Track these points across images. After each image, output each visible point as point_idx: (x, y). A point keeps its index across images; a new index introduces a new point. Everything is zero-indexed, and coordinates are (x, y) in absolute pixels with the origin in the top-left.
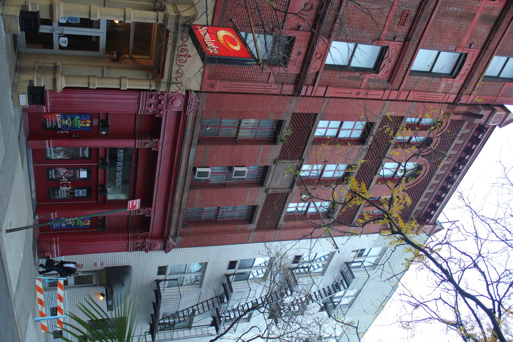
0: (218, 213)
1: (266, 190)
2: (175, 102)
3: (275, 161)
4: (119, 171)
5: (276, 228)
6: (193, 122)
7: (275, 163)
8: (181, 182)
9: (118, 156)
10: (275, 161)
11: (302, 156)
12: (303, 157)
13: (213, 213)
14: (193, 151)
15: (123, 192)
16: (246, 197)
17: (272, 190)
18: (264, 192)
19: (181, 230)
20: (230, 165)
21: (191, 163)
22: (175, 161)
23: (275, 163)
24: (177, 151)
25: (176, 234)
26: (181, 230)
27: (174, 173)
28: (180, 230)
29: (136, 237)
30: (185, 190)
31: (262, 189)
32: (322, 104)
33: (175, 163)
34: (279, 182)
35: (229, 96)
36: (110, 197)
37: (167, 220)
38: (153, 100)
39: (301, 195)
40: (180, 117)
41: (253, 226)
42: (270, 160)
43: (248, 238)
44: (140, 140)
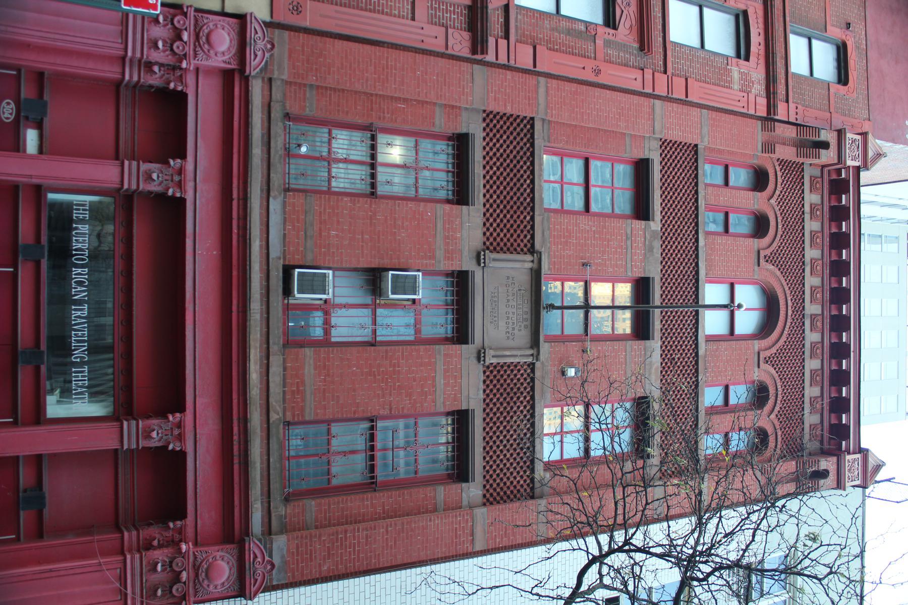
0: (372, 458)
1: (479, 353)
2: (214, 38)
3: (478, 255)
4: (79, 302)
5: (532, 497)
6: (265, 117)
7: (479, 264)
8: (258, 316)
9: (75, 245)
10: (478, 255)
11: (533, 245)
12: (537, 246)
13: (360, 466)
14: (275, 205)
15: (95, 394)
16: (434, 378)
17: (492, 352)
18: (475, 361)
19: (282, 510)
22: (235, 230)
23: (479, 264)
24: (235, 195)
25: (268, 531)
26: (282, 510)
27: (235, 273)
28: (279, 510)
29: (149, 547)
30: (274, 348)
31: (467, 350)
32: (537, 92)
33: (235, 237)
34: (502, 324)
35: (339, 44)
36: (55, 408)
37: (236, 461)
38: (160, 32)
39: (563, 373)
40: (233, 79)
41: (473, 491)
42: (465, 253)
43: (472, 534)
44: (135, 163)
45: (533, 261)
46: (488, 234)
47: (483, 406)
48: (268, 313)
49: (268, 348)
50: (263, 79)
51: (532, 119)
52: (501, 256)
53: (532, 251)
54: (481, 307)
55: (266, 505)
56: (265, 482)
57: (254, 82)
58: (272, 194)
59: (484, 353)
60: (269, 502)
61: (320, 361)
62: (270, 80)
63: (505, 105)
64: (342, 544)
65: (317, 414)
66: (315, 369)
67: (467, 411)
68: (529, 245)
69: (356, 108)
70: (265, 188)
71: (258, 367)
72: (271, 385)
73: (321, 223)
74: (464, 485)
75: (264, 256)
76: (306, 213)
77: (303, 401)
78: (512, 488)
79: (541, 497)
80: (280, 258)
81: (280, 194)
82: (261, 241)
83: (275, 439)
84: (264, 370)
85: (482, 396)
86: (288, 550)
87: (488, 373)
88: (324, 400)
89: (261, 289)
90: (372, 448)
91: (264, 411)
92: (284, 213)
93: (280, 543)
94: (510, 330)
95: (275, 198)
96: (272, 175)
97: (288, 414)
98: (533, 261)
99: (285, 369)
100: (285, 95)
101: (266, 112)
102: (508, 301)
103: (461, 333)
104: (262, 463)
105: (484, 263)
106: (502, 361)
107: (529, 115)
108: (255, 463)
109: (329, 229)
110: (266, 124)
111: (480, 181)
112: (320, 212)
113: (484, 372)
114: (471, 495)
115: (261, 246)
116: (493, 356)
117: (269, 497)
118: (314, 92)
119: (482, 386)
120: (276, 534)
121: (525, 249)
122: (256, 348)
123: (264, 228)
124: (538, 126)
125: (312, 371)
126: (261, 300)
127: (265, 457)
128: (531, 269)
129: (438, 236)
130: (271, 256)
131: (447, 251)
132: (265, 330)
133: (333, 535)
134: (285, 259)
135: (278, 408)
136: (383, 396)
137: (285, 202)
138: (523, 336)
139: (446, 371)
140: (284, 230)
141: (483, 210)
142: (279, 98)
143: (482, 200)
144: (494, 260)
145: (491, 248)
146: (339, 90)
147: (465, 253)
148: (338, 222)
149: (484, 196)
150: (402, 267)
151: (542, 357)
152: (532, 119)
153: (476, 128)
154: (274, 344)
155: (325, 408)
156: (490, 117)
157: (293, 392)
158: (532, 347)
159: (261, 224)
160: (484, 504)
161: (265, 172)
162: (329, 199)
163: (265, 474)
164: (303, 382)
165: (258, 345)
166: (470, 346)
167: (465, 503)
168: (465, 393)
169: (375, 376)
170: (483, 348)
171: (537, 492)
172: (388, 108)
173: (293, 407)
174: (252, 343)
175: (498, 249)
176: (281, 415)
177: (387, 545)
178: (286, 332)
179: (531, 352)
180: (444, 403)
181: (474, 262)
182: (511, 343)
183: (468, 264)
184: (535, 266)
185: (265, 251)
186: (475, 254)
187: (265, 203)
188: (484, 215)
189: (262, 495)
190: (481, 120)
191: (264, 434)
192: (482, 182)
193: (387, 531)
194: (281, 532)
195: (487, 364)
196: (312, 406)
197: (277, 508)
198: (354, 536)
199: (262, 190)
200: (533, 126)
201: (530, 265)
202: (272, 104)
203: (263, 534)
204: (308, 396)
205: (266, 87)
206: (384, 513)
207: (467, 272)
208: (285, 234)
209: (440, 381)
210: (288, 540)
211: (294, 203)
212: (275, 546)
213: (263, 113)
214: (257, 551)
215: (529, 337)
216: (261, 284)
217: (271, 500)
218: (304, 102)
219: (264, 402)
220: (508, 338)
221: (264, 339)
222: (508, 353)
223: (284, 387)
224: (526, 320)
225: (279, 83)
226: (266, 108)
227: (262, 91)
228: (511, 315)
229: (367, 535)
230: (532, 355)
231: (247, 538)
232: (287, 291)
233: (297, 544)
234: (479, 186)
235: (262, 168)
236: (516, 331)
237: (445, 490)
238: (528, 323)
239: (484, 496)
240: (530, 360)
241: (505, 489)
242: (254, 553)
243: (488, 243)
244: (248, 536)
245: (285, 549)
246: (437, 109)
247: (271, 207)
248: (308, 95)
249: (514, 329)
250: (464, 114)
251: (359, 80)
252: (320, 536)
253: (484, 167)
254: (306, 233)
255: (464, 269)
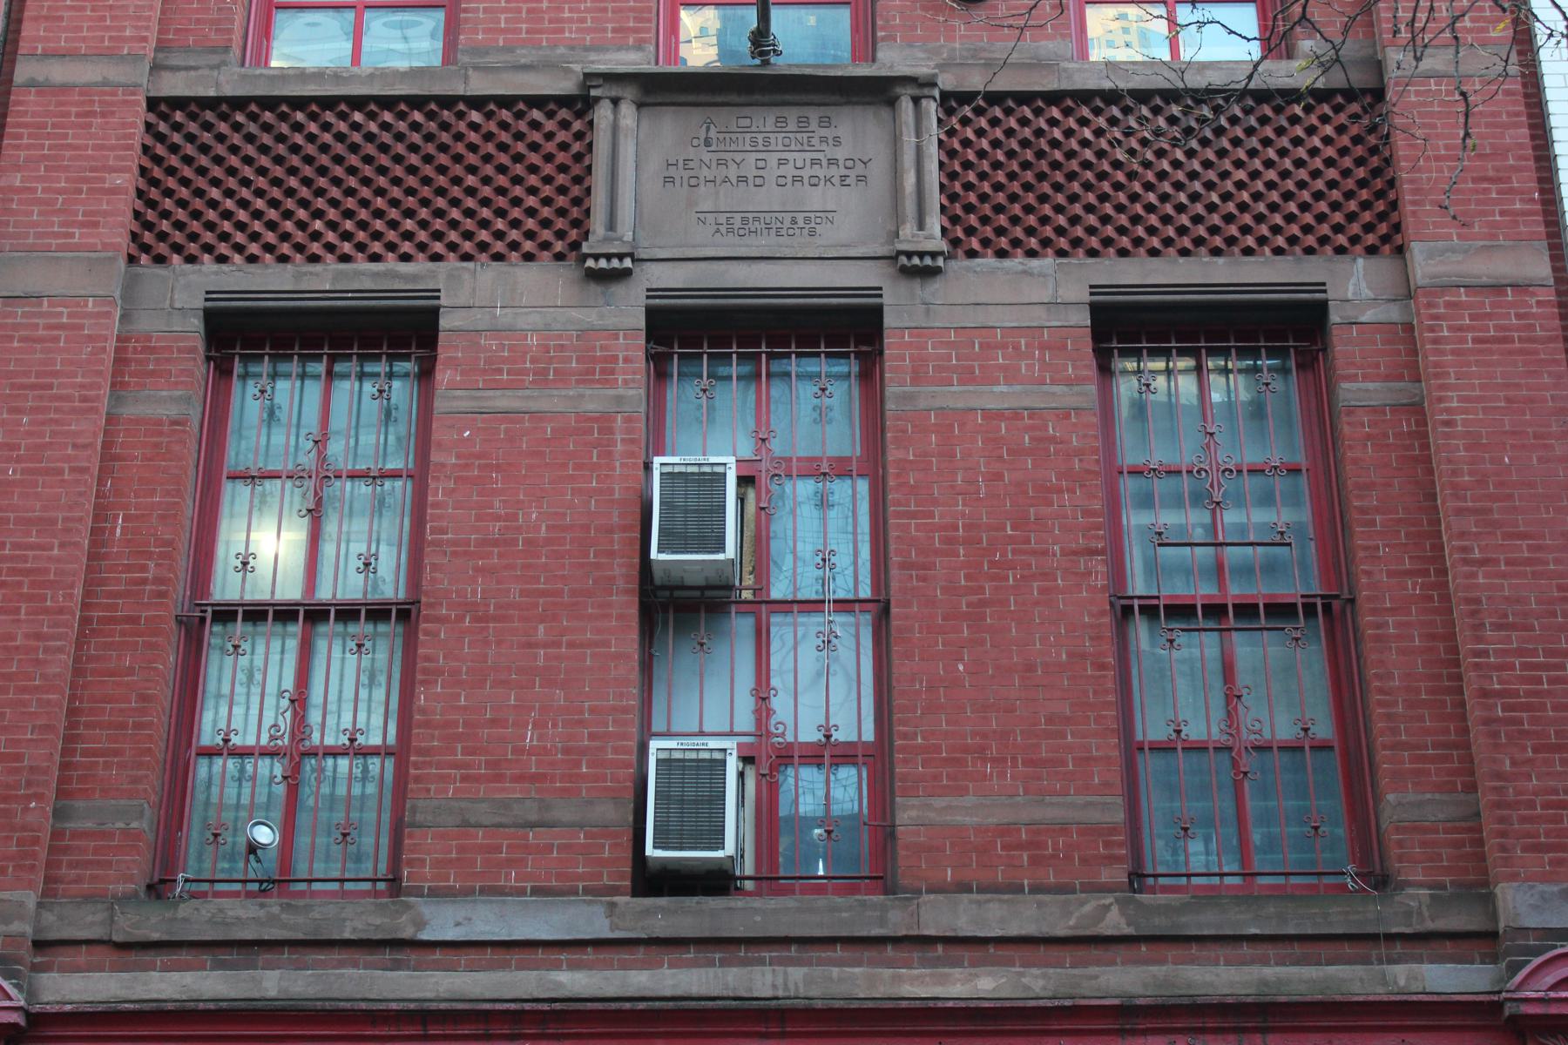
0: (1246, 610)
1: (909, 273)
5: (1378, 94)
6: (160, 959)
7: (626, 274)
8: (797, 974)
11: (563, 101)
13: (1273, 650)
14: (443, 922)
17: (908, 230)
18: (936, 285)
20: (626, 606)
21: (591, 921)
23: (626, 274)
25: (1484, 941)
28: (1414, 905)
30: (897, 921)
32: (65, 88)
34: (816, 199)
41: (1354, 287)
42: (590, 317)
43: (1497, 288)
45: (615, 102)
46: (528, 246)
47: (1079, 259)
48: (786, 941)
49: (896, 941)
50: (36, 968)
51: (153, 104)
52: (599, 201)
53: (580, 104)
54: (763, 265)
55: (1398, 948)
56: (1326, 950)
57: (47, 996)
58: (407, 933)
59: (909, 255)
60: (1391, 938)
61: (936, 777)
62: (40, 945)
63: (114, 191)
64: (1528, 707)
65: (1105, 784)
66: (963, 792)
67: (1095, 309)
68: (564, 114)
69: (130, 671)
70: (387, 955)
71: (957, 972)
72: (1014, 930)
73: (499, 778)
74: (1334, 317)
75: (605, 955)
76: (466, 824)
77: (1063, 828)
78: (1347, 162)
79: (1378, 67)
80: (613, 905)
81: (408, 907)
82: (557, 966)
83: (1183, 919)
84: (965, 953)
85: (1047, 262)
86: (1545, 878)
87: (975, 244)
88: (1064, 763)
89: (711, 964)
90: (1215, 611)
91: (1095, 952)
92: (467, 892)
93: (1520, 904)
94: (835, 172)
95: (420, 924)
96: (347, 935)
97: (1106, 875)
98: (615, 102)
99: (963, 888)
100: (89, 898)
101: (147, 957)
102: (742, 179)
103: (845, 330)
104: (1265, 961)
105: (621, 257)
106: (935, 198)
107: (140, 115)
108: (1264, 982)
109: (518, 751)
110: (184, 956)
111: (358, 274)
112: (464, 779)
113: (971, 254)
114: (1367, 293)
115: (574, 966)
116: (921, 225)
117: (1373, 938)
118: (80, 804)
119: (1017, 262)
120: (1494, 917)
121: (577, 125)
122: (897, 979)
123: (516, 956)
124: (175, 85)
125: (970, 800)
126: (745, 963)
127: (1246, 950)
128: (640, 105)
129: (533, 406)
130: (608, 934)
131: (586, 377)
132: (839, 952)
133: (1495, 735)
134: (615, 891)
135: (1087, 908)
136: (1047, 575)
137: (434, 893)
138: (855, 134)
139: (968, 377)
140: (521, 892)
141: (452, 261)
142: (100, 917)
143: (420, 266)
144: (611, 225)
145: (574, 234)
146: (72, 725)
147: (590, 317)
148: (494, 722)
149: (406, 258)
150: (636, 522)
151: (923, 70)
152: (153, 104)
153: (189, 287)
154: (882, 922)
155: (1086, 760)
156: (155, 238)
157: (1034, 861)
158: (892, 103)
159: (504, 966)
160: (1400, 250)
161: (336, 955)
162: (420, 752)
163: (1297, 949)
164: (1005, 830)
165: (887, 972)
166: (887, 300)
167: (1394, 313)
168: (1038, 317)
169: (983, 603)
170: (894, 258)
171: (1359, 79)
172: (128, 568)
173: (1083, 861)
174: (881, 991)
175: (575, 212)
176: (1109, 899)
177: (1529, 562)
178: (846, 884)
179: (906, 105)
180: (1069, 382)
181: (618, 290)
182: (878, 171)
183: (626, 311)
184: (629, 93)
185: (590, 954)
186: (595, 288)
187: (438, 955)
188: (466, 257)
189: (1366, 961)
190: (159, 271)
191: (1172, 952)
192: (362, 265)
193: (1483, 562)
194: (1488, 900)
195: (944, 246)
196: (1080, 800)
197: (1408, 914)
198: (1501, 667)
199: (397, 966)
200: (179, 103)
201: (627, 112)
202: (115, 938)
203: (1494, 959)
204: (1051, 812)
205: (64, 957)
206: (1425, 573)
207: (651, 313)
208: (536, 891)
209: (999, 396)
210: (1514, 877)
211: (437, 863)
212: (1532, 921)
213: (150, 967)
214: (1550, 979)
215: (859, 109)
216: (694, 964)
217: (1382, 930)
218: (104, 835)
219: (1067, 954)
220: (861, 178)
221: (868, 953)
222: (910, 180)
223: (1019, 889)
224: (803, 121)
225: (49, 918)
226: (133, 957)
227: (77, 969)
228: (789, 170)
229: (1498, 627)
230: (916, 101)
231: (1508, 1010)
232: (717, 881)
233: (1525, 849)
234: (377, 275)
235: (323, 965)
236: (840, 154)
237: (1352, 378)
238: (813, 114)
239: (1371, 251)
240: (932, 108)
241: (1350, 184)
242: (1553, 987)
243: (559, 246)
244: (1498, 1006)
245: (1541, 887)
246: (129, 410)
247: (450, 935)
248: (89, 825)
249: (832, 162)
250: (145, 323)
251: (38, 662)
252: (1499, 776)
253: (314, 259)
254: (532, 825)
255: (642, 323)
